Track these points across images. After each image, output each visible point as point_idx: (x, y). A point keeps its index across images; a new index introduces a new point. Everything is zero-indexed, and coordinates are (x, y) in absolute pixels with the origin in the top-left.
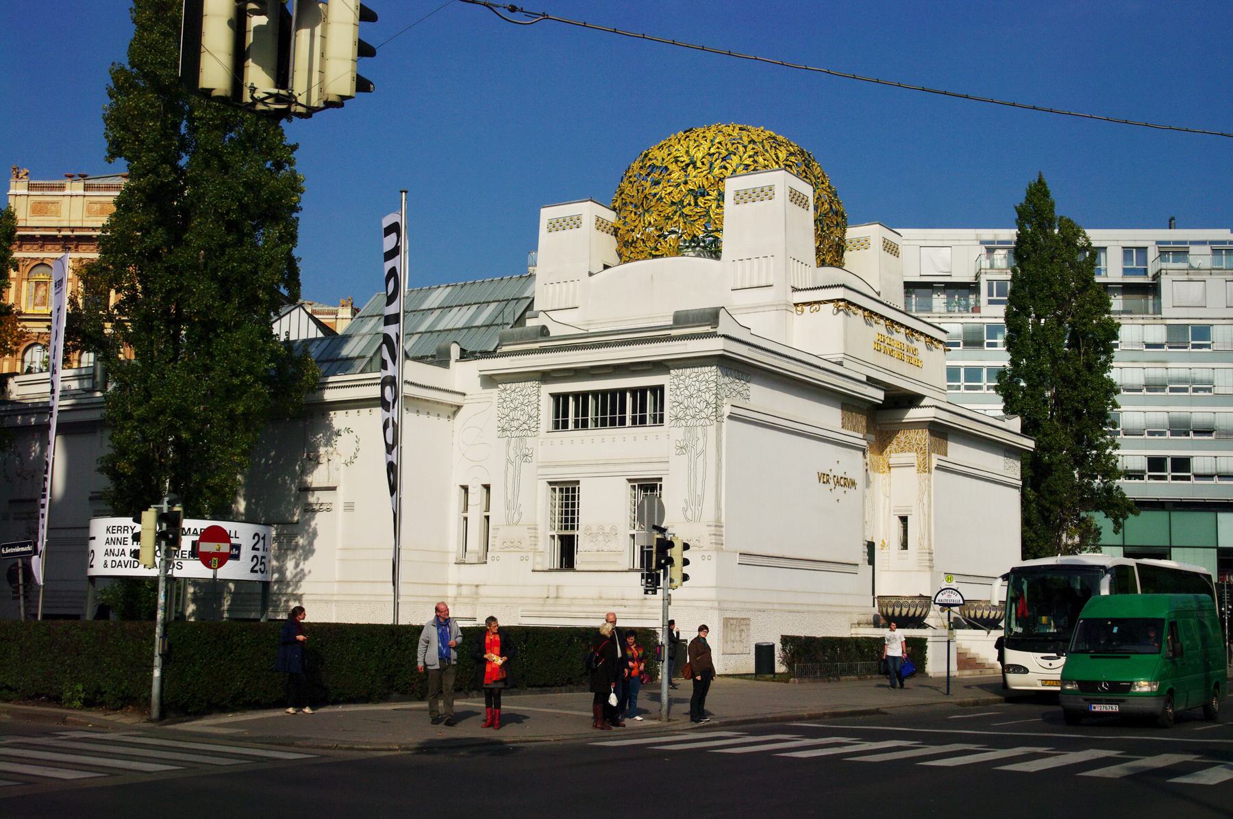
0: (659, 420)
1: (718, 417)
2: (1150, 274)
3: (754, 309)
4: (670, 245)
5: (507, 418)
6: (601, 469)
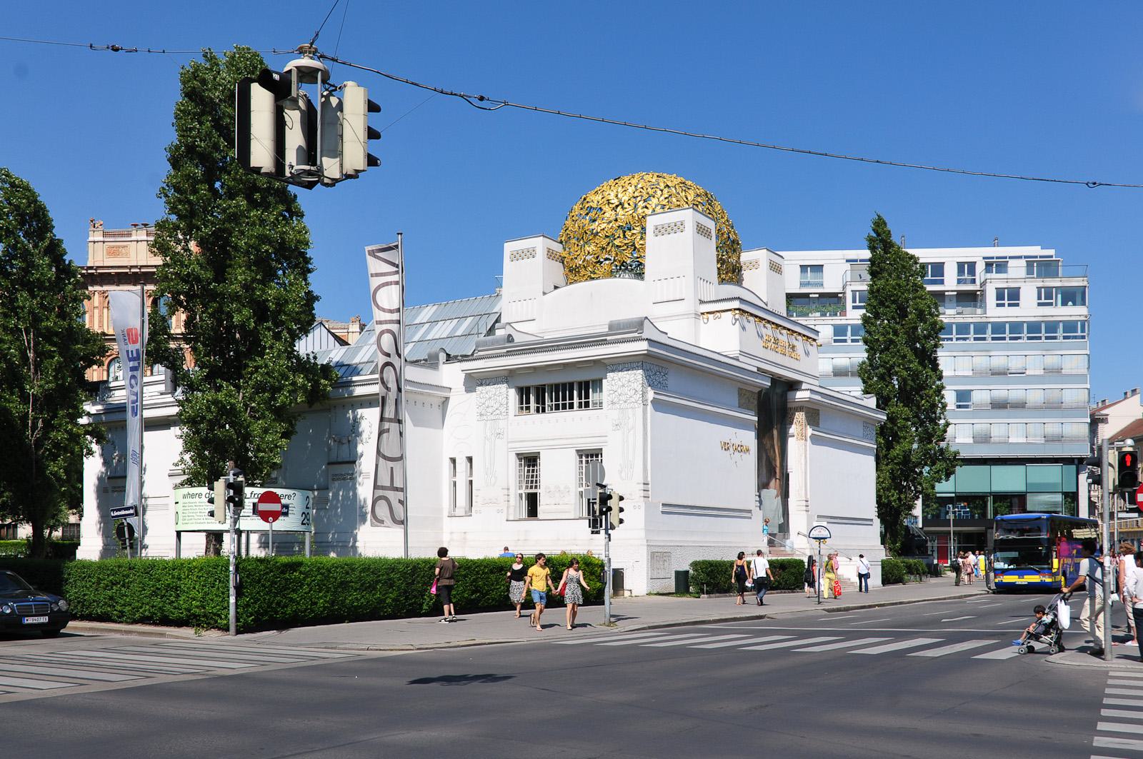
2: (978, 282)
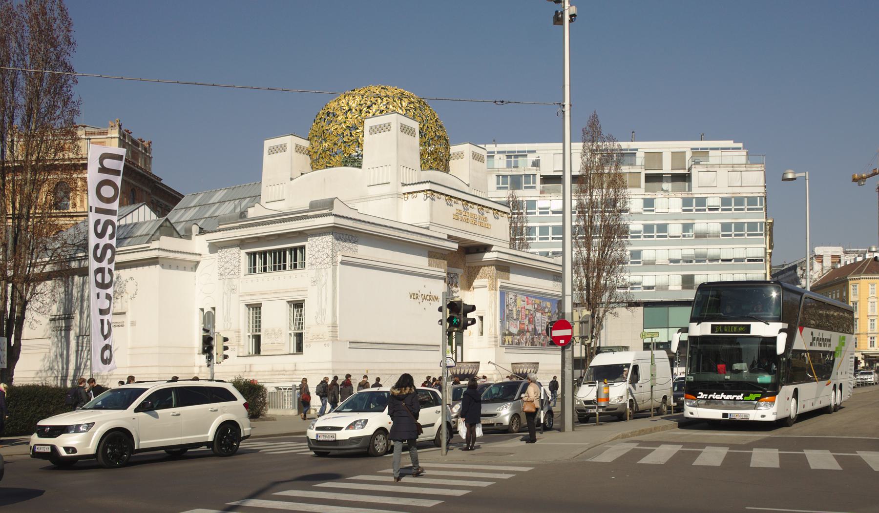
0: (303, 266)
1: (334, 263)
3: (380, 197)
4: (337, 160)
6: (273, 296)
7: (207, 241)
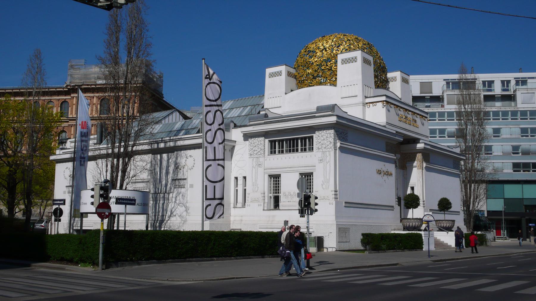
0: (311, 149)
4: (317, 81)
5: (252, 150)
7: (242, 132)
